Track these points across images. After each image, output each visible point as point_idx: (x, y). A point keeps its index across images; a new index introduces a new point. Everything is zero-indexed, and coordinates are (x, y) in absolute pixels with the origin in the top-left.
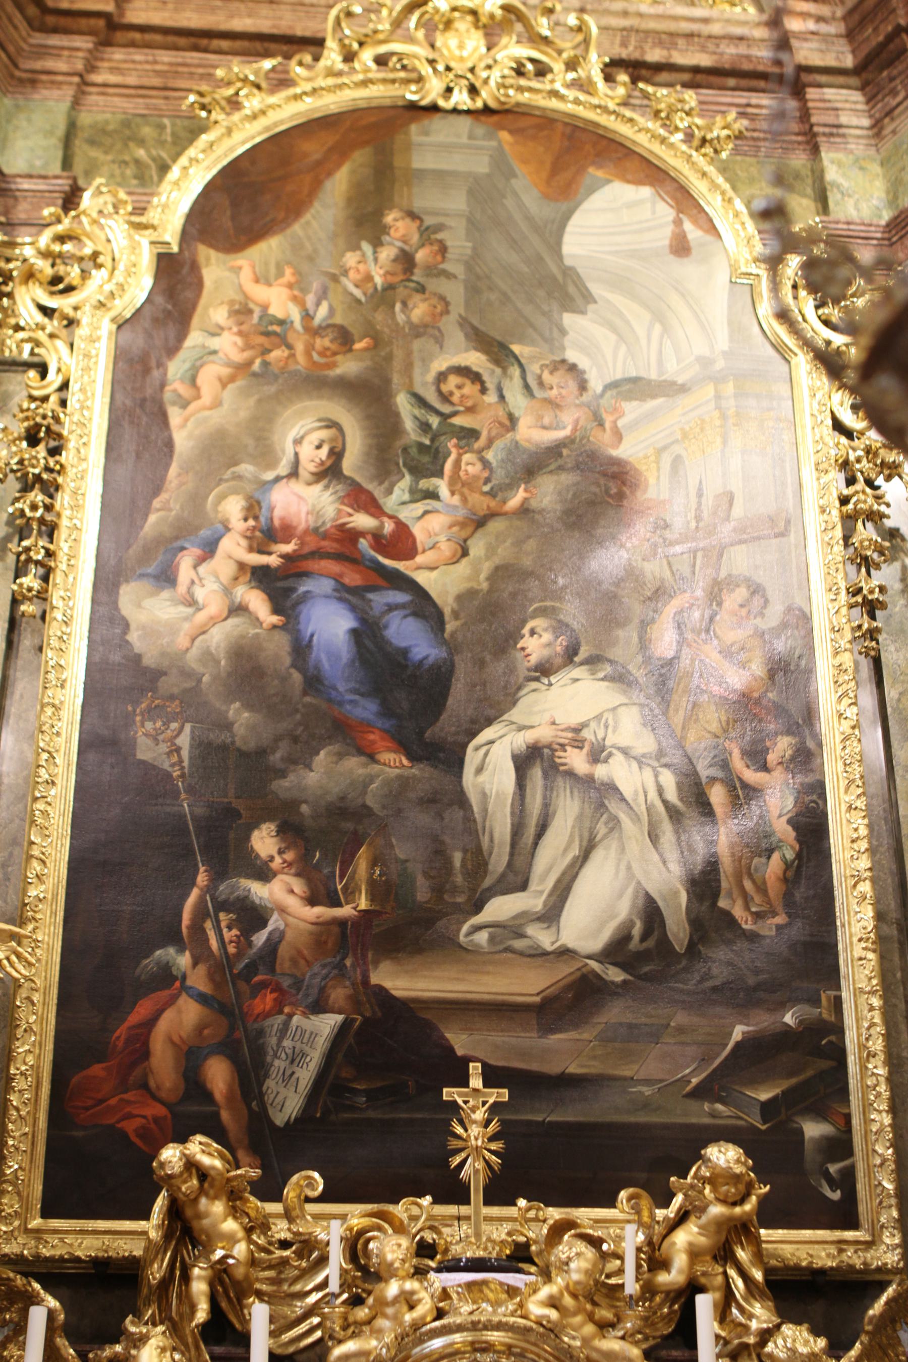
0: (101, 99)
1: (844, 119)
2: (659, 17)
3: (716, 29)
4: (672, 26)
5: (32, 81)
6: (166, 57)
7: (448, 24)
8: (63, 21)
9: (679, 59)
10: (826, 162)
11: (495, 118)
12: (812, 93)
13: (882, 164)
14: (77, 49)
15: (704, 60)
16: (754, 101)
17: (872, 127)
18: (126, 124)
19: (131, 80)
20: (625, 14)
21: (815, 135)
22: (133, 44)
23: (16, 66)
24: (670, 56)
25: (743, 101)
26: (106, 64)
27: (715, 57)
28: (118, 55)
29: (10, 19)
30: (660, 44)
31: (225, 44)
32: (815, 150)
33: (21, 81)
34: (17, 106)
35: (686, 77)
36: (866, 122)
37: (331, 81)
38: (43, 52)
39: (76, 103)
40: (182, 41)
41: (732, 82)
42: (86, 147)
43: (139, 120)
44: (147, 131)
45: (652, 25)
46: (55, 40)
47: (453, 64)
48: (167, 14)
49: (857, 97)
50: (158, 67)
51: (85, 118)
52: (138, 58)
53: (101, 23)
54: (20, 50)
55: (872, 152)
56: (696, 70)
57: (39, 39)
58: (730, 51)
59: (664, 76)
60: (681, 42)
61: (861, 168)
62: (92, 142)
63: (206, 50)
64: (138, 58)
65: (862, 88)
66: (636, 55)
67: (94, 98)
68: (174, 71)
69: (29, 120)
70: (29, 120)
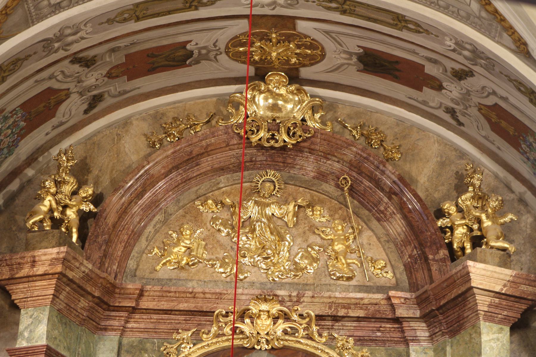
0: (131, 333)
1: (418, 334)
2: (343, 298)
3: (366, 301)
4: (349, 302)
5: (105, 329)
6: (155, 316)
7: (259, 317)
8: (116, 308)
9: (352, 314)
10: (411, 352)
11: (276, 351)
12: (405, 324)
13: (434, 351)
14: (122, 317)
15: (361, 313)
16: (383, 325)
17: (429, 336)
18: (141, 342)
19: (142, 326)
20: (330, 297)
21: (407, 340)
22: (143, 313)
23: (99, 324)
24: (348, 313)
25: (379, 325)
26: (132, 320)
27: (366, 312)
28: (137, 316)
29: (97, 311)
30: (344, 307)
31: (177, 313)
32: (408, 345)
33: (101, 329)
34: (99, 338)
35: (355, 319)
36: (427, 334)
37: (214, 341)
38: (109, 318)
39: (122, 335)
40: (161, 312)
41: (373, 320)
42: (125, 354)
43: (145, 340)
44: (148, 346)
45: (340, 301)
46: (113, 314)
47: (260, 332)
48: (155, 303)
49: (424, 325)
50: (152, 320)
51: (125, 341)
52: (144, 317)
53: (131, 309)
54: (100, 319)
55: (430, 345)
56: (358, 317)
57: (107, 313)
58: (372, 308)
59: (346, 319)
60: (352, 306)
61: (425, 353)
62: (128, 352)
63: (170, 314)
64: (144, 317)
65: (425, 322)
66: (334, 313)
67: (128, 334)
68: (158, 322)
69: (104, 345)
70: (104, 345)
